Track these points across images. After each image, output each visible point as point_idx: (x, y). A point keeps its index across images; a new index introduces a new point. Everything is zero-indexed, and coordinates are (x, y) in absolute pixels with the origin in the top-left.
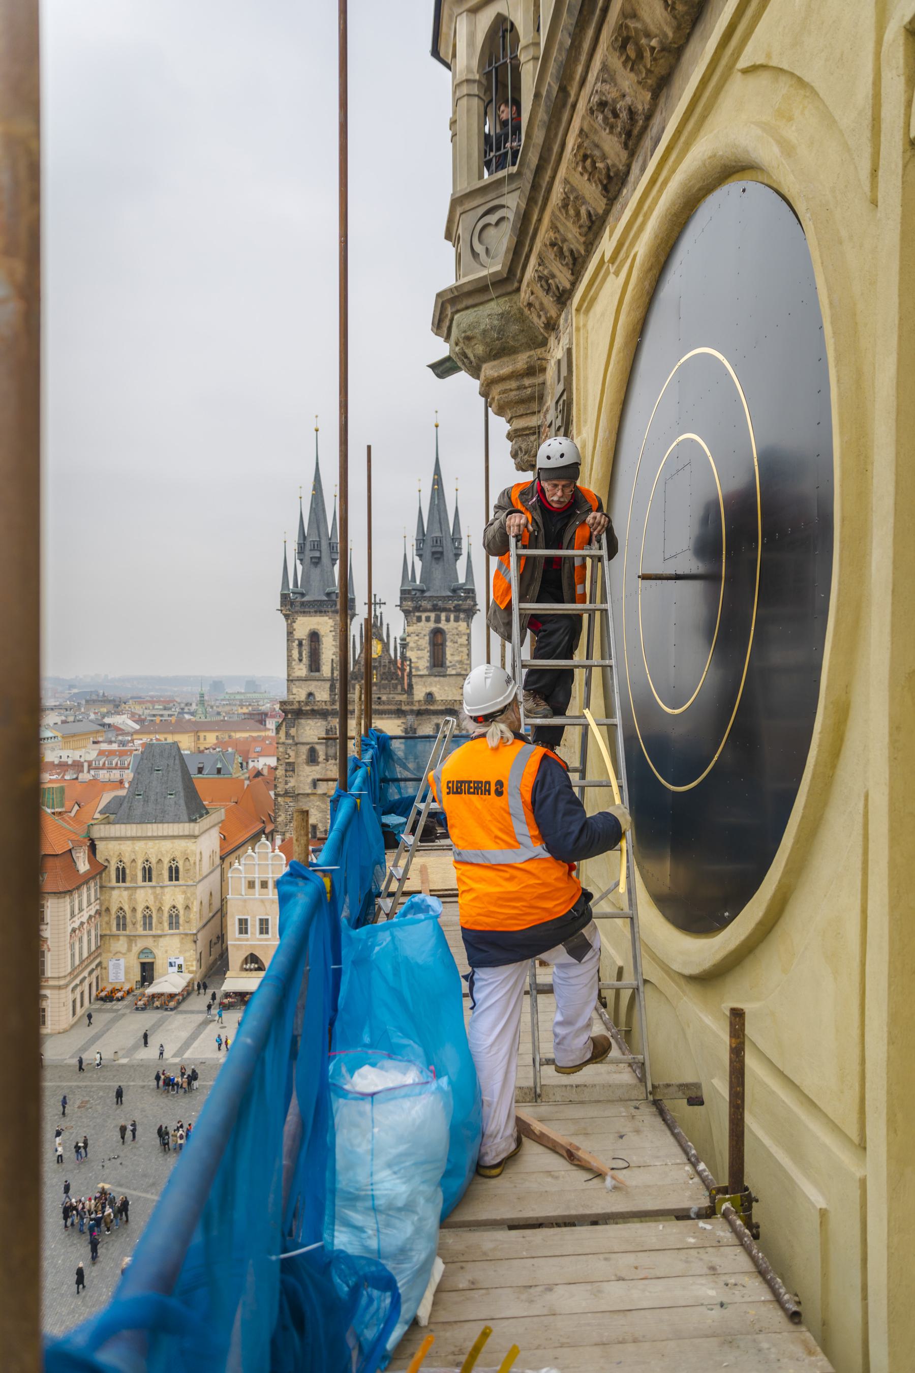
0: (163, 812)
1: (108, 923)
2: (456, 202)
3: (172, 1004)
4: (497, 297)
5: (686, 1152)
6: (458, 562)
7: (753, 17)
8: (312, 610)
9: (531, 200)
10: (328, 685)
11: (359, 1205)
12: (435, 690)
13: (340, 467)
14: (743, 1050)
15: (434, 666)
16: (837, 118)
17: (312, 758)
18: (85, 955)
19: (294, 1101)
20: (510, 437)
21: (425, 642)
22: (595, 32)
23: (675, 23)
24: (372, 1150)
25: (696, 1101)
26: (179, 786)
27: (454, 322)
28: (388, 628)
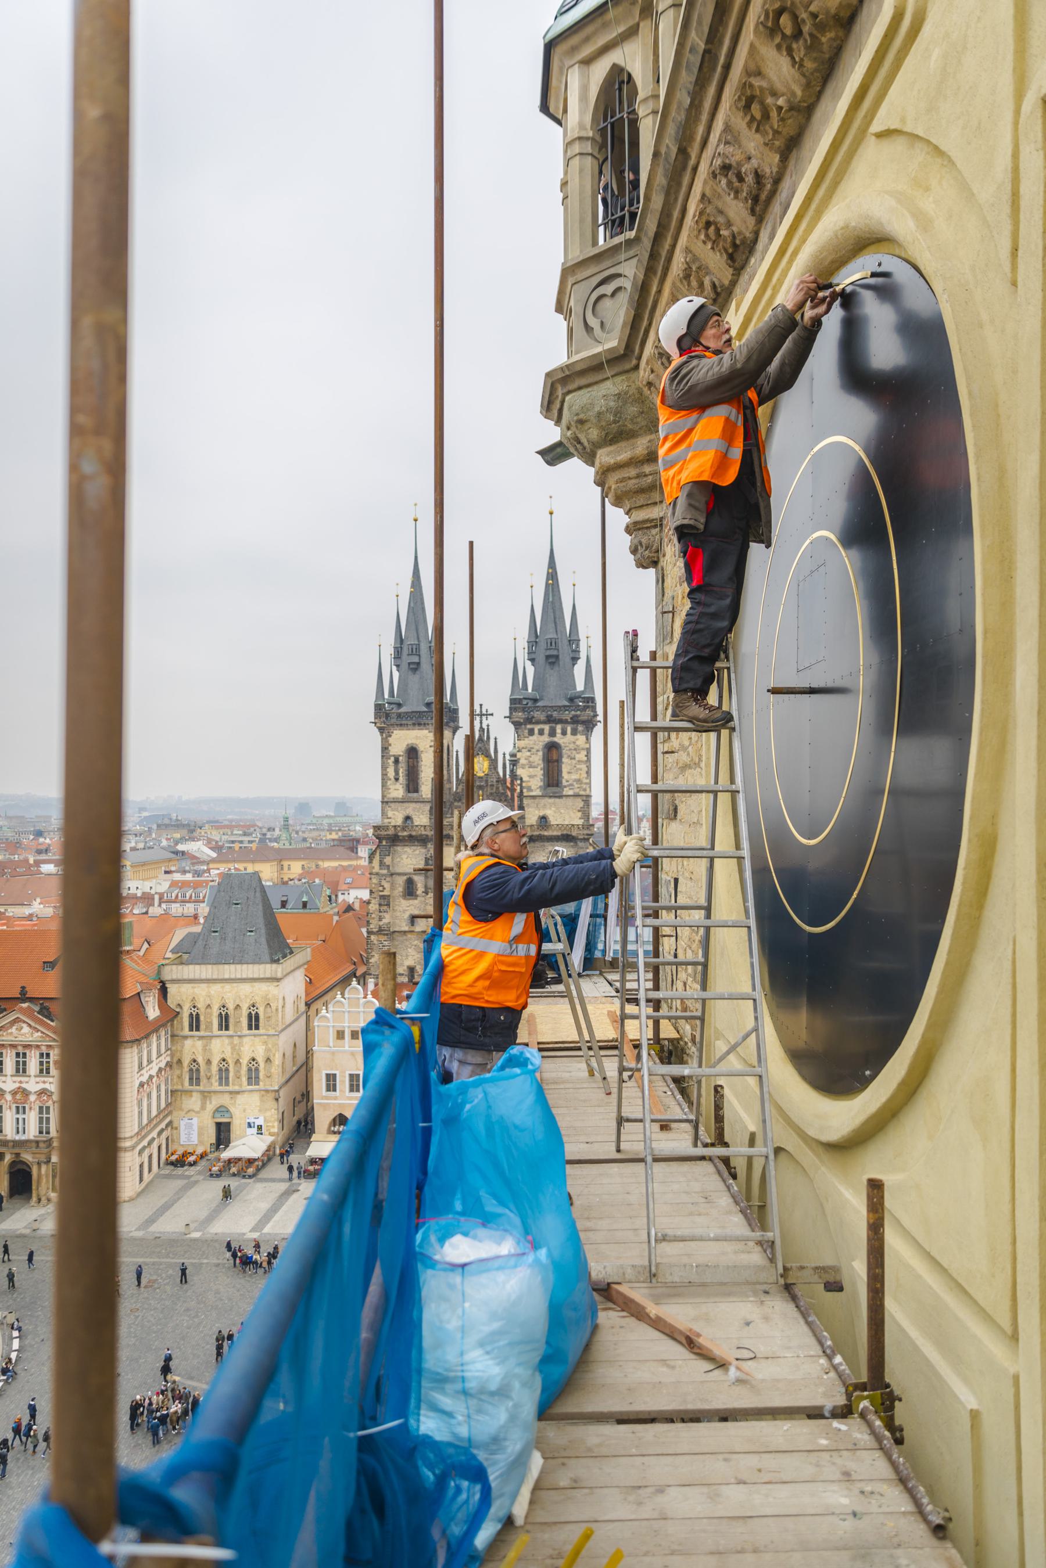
1: (180, 1077)
2: (567, 272)
3: (251, 1171)
5: (821, 1343)
7: (886, 78)
8: (410, 723)
9: (650, 270)
11: (449, 1387)
12: (549, 813)
13: (436, 572)
14: (882, 1226)
15: (549, 786)
16: (975, 192)
17: (410, 891)
18: (154, 1113)
19: (378, 1271)
20: (628, 530)
21: (538, 758)
23: (803, 81)
24: (463, 1326)
25: (835, 1286)
26: (260, 922)
28: (496, 743)
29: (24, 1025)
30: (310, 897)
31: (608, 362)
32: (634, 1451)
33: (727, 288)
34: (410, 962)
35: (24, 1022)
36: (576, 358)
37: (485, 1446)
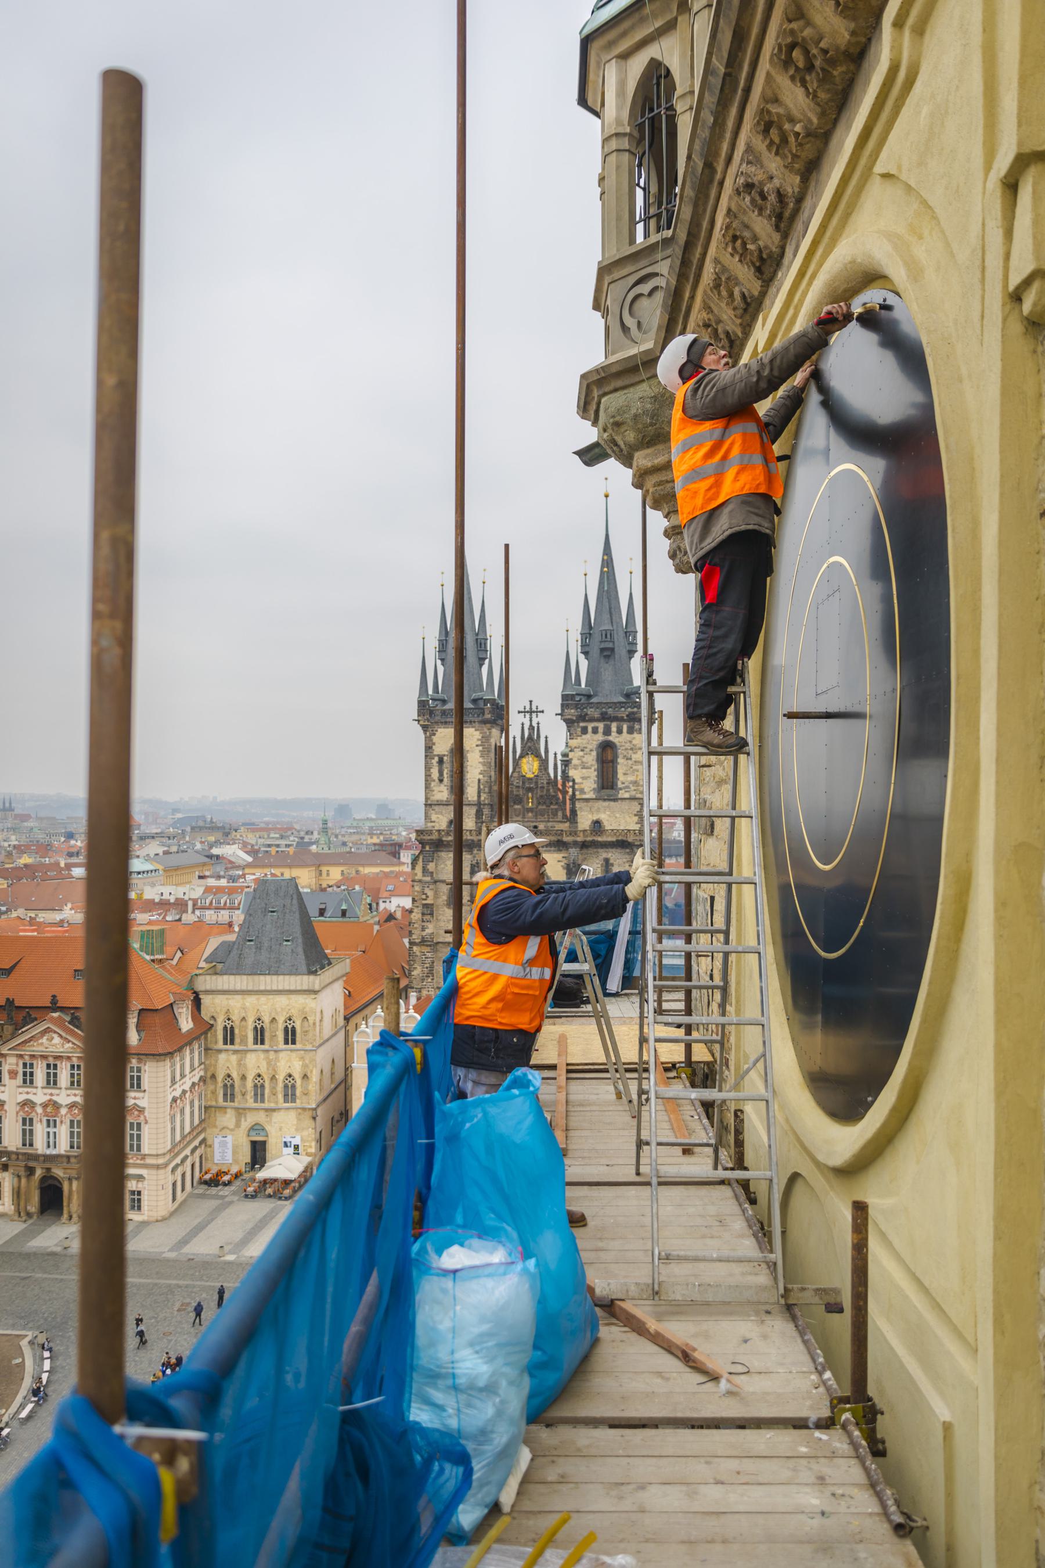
0: (279, 961)
1: (214, 1092)
2: (604, 270)
3: (287, 1192)
5: (814, 1361)
7: (888, 121)
9: (682, 277)
11: (440, 1382)
12: (603, 817)
14: (866, 1246)
15: (603, 788)
18: (187, 1129)
19: (375, 1274)
21: (591, 759)
22: (738, 112)
23: (818, 110)
24: (454, 1327)
26: (297, 931)
27: (602, 406)
28: (546, 741)
29: (55, 1036)
30: (349, 905)
32: (621, 1452)
33: (757, 299)
35: (55, 1032)
36: (613, 359)
37: (474, 1437)
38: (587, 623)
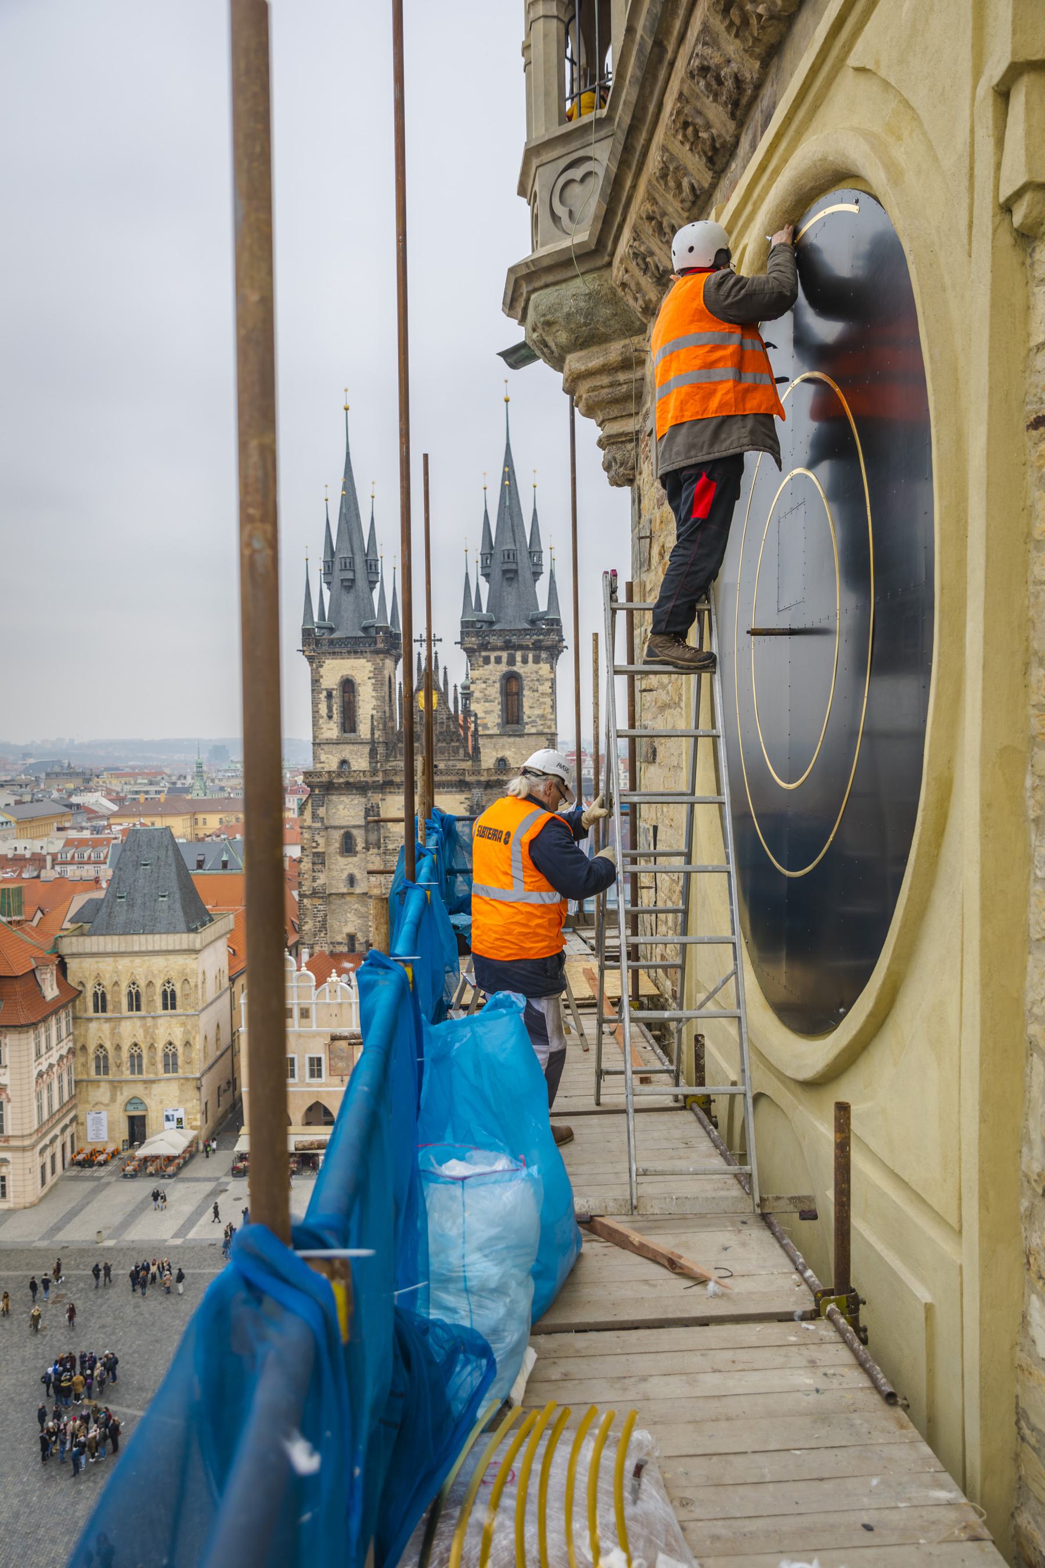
1: (85, 1065)
2: (531, 153)
3: (171, 1170)
4: (582, 274)
5: (794, 1261)
6: (538, 582)
7: (863, 12)
9: (623, 163)
10: (366, 749)
11: (451, 1286)
12: (508, 754)
13: (402, 506)
15: (508, 723)
17: (348, 847)
18: (56, 1106)
20: (601, 444)
21: (494, 691)
25: (809, 1215)
26: (174, 885)
28: (445, 673)
30: (231, 856)
31: (578, 257)
32: (619, 1351)
33: (707, 191)
34: (349, 929)
36: (542, 252)
38: (487, 542)
